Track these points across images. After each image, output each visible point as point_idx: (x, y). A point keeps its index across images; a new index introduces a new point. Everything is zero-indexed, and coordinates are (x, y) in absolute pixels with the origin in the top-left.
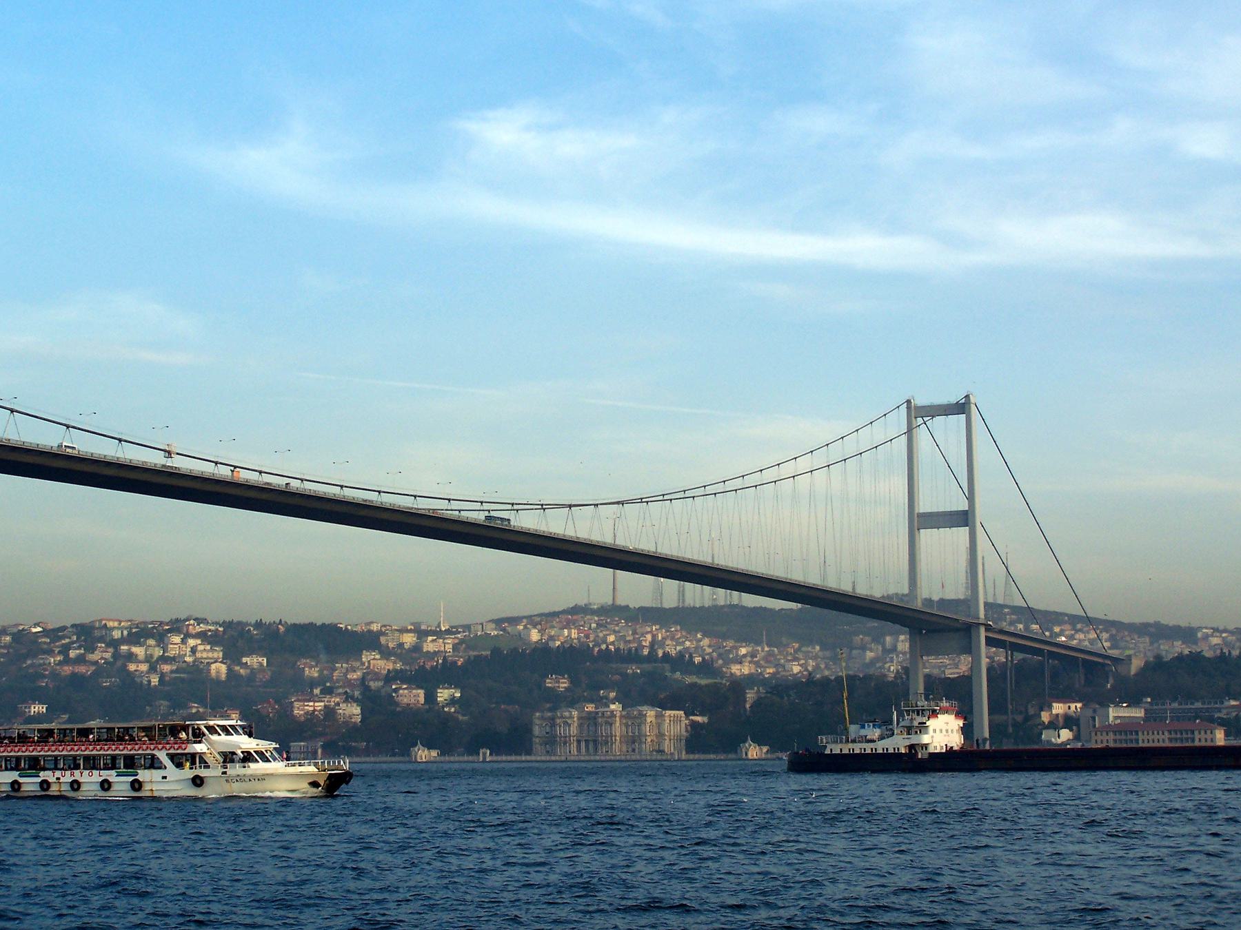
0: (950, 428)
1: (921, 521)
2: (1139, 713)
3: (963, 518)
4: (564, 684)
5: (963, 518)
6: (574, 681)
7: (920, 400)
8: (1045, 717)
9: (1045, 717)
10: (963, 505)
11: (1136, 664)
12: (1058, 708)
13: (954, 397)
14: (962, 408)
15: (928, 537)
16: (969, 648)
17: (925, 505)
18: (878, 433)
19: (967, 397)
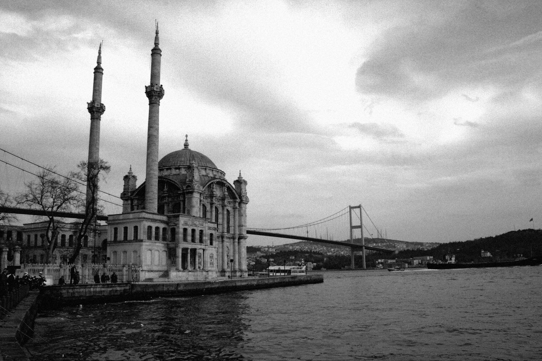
0: (358, 210)
1: (352, 227)
2: (394, 261)
3: (360, 227)
4: (293, 258)
5: (360, 227)
6: (295, 257)
7: (352, 205)
8: (377, 262)
9: (377, 262)
10: (360, 225)
11: (397, 252)
12: (380, 261)
13: (357, 205)
14: (359, 207)
15: (354, 230)
16: (362, 251)
17: (354, 225)
18: (344, 212)
19: (360, 205)
